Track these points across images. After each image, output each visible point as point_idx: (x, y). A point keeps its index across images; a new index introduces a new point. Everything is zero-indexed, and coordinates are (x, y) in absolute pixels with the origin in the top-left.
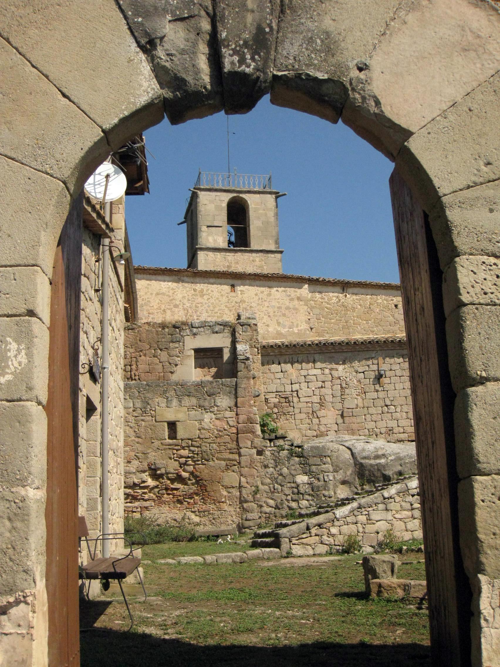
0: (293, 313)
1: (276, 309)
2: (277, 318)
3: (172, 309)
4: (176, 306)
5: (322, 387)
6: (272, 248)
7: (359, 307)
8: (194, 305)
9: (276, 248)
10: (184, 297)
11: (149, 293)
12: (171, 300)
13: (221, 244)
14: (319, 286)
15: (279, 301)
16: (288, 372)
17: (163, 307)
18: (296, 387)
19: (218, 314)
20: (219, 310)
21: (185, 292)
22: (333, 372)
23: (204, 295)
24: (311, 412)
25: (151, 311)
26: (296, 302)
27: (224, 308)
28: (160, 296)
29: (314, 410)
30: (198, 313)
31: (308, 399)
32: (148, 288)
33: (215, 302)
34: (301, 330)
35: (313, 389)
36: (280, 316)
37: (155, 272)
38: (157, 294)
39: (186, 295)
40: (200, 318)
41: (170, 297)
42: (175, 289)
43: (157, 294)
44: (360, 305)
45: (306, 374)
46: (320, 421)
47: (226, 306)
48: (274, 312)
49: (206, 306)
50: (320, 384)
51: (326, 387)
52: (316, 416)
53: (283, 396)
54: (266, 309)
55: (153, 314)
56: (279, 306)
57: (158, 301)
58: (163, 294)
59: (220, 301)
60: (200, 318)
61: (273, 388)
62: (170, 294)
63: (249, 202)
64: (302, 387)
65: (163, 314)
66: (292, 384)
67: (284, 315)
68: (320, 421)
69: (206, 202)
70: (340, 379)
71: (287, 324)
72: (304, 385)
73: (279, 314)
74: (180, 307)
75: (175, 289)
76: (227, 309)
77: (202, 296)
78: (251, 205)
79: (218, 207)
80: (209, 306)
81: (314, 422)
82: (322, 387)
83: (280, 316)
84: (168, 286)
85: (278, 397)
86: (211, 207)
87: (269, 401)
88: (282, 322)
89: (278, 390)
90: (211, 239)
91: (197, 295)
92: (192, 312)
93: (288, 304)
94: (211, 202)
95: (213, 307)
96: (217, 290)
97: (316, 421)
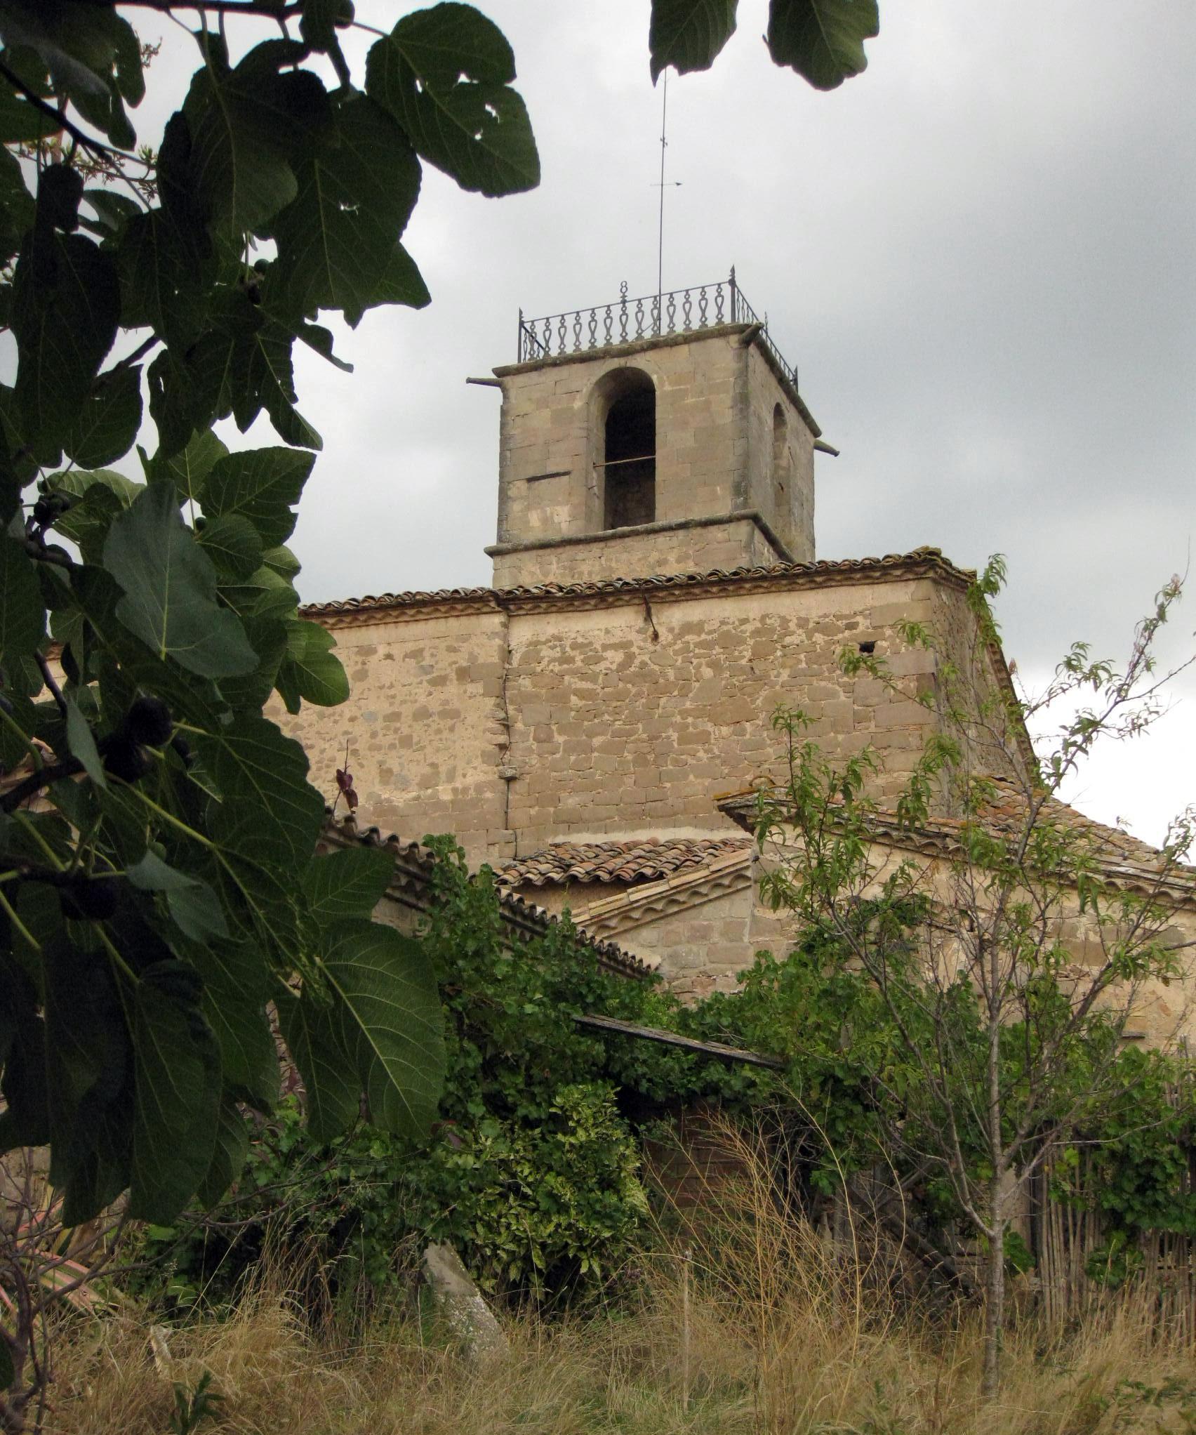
0: (439, 731)
1: (379, 724)
2: (379, 757)
6: (723, 511)
7: (708, 672)
9: (736, 507)
13: (564, 526)
14: (553, 618)
15: (392, 692)
26: (452, 689)
34: (465, 790)
36: (392, 746)
44: (714, 665)
48: (374, 735)
54: (346, 726)
56: (390, 710)
63: (655, 378)
67: (406, 742)
69: (527, 407)
71: (416, 771)
73: (391, 738)
78: (662, 385)
79: (561, 417)
83: (392, 746)
86: (541, 420)
88: (396, 769)
90: (534, 518)
93: (422, 699)
94: (542, 403)
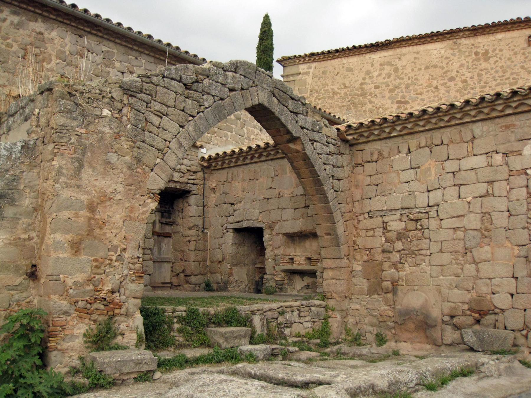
3: (446, 83)
4: (452, 79)
5: (487, 194)
8: (476, 74)
10: (462, 66)
11: (416, 69)
12: (445, 72)
16: (423, 168)
17: (435, 83)
18: (435, 197)
19: (511, 80)
20: (512, 74)
21: (463, 58)
22: (511, 159)
23: (490, 57)
24: (462, 250)
25: (419, 92)
27: (520, 70)
28: (431, 69)
29: (468, 245)
30: (482, 83)
31: (456, 223)
32: (414, 63)
33: (504, 64)
35: (469, 199)
37: (422, 40)
38: (427, 68)
39: (465, 62)
40: (484, 89)
41: (443, 68)
42: (450, 58)
43: (427, 68)
45: (456, 169)
46: (478, 271)
47: (522, 67)
49: (492, 72)
50: (482, 188)
51: (496, 193)
52: (470, 259)
53: (412, 217)
55: (421, 94)
57: (428, 76)
58: (435, 66)
59: (513, 62)
60: (484, 89)
61: (396, 200)
62: (444, 65)
64: (446, 198)
65: (434, 92)
66: (429, 191)
68: (478, 271)
70: (526, 174)
72: (452, 192)
74: (457, 79)
75: (450, 58)
76: (522, 71)
77: (487, 59)
80: (497, 72)
81: (466, 271)
82: (487, 194)
84: (440, 55)
85: (405, 218)
87: (389, 228)
89: (405, 206)
91: (479, 60)
92: (474, 84)
95: (502, 71)
96: (507, 47)
97: (470, 269)
